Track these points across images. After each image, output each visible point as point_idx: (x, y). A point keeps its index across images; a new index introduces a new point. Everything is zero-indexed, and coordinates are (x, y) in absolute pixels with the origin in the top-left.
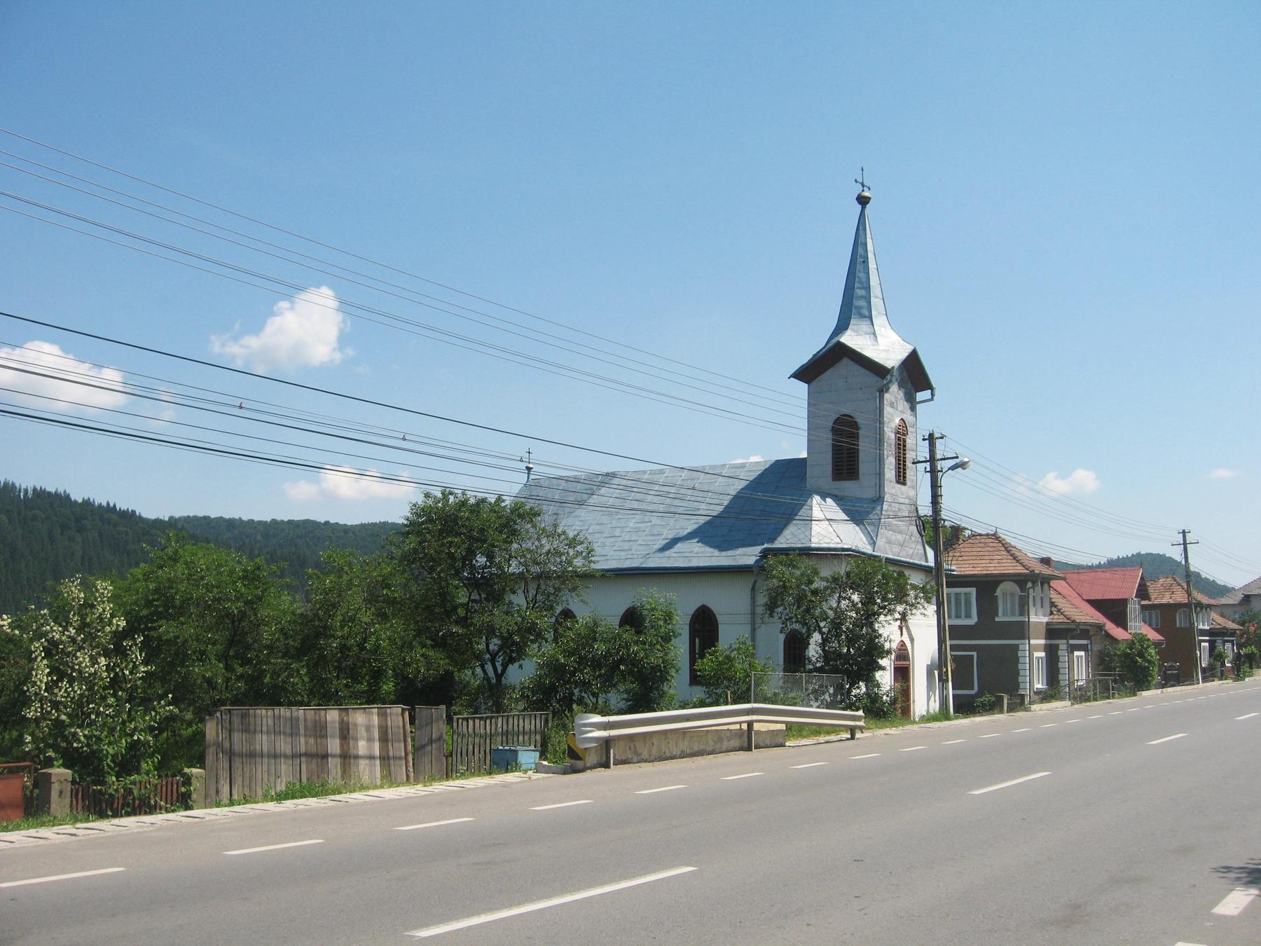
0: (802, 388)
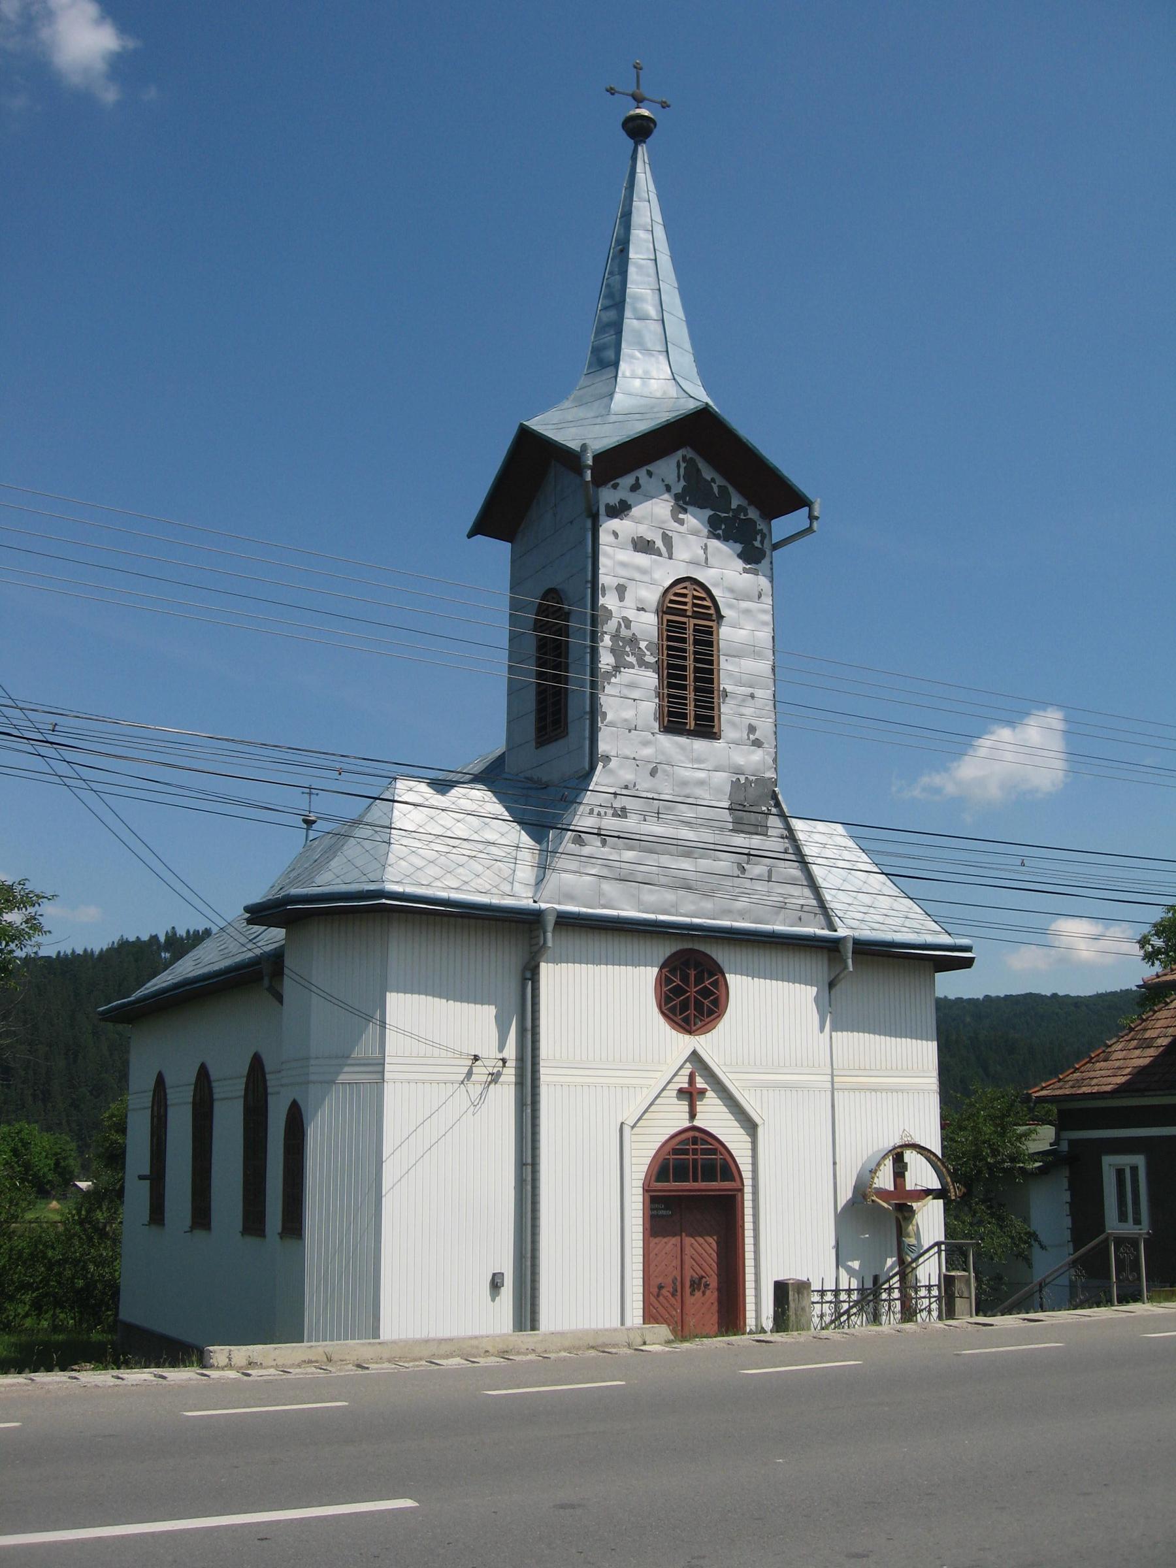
0: (500, 550)
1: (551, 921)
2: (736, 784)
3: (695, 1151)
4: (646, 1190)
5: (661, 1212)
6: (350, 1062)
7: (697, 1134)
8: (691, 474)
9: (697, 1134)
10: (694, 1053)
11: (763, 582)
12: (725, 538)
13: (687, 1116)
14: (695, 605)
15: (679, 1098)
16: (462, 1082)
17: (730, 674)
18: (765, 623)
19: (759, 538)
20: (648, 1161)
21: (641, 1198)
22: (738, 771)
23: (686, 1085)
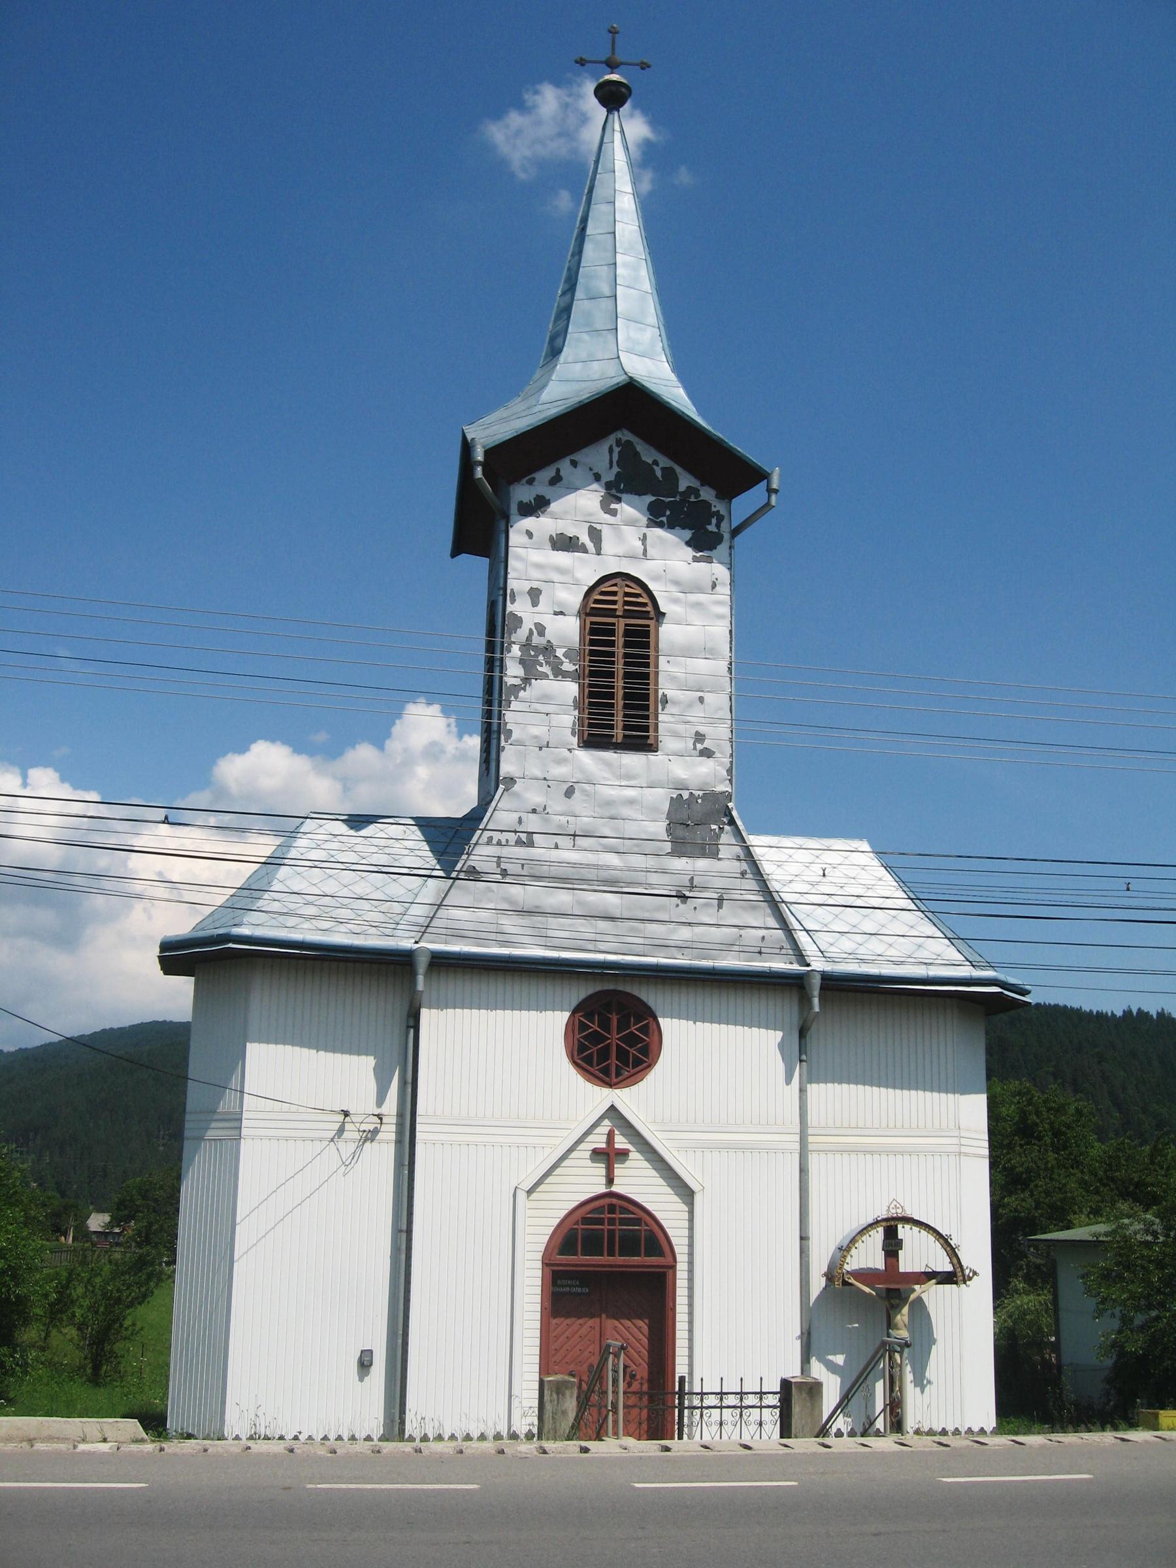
2: (676, 802)
3: (612, 1221)
4: (546, 1263)
6: (216, 1117)
7: (614, 1201)
8: (628, 457)
9: (614, 1201)
10: (612, 1108)
11: (719, 571)
12: (671, 526)
13: (603, 1180)
14: (626, 603)
16: (332, 1140)
17: (673, 679)
18: (720, 617)
19: (714, 521)
20: (550, 1230)
21: (539, 1273)
22: (680, 786)
23: (604, 1146)
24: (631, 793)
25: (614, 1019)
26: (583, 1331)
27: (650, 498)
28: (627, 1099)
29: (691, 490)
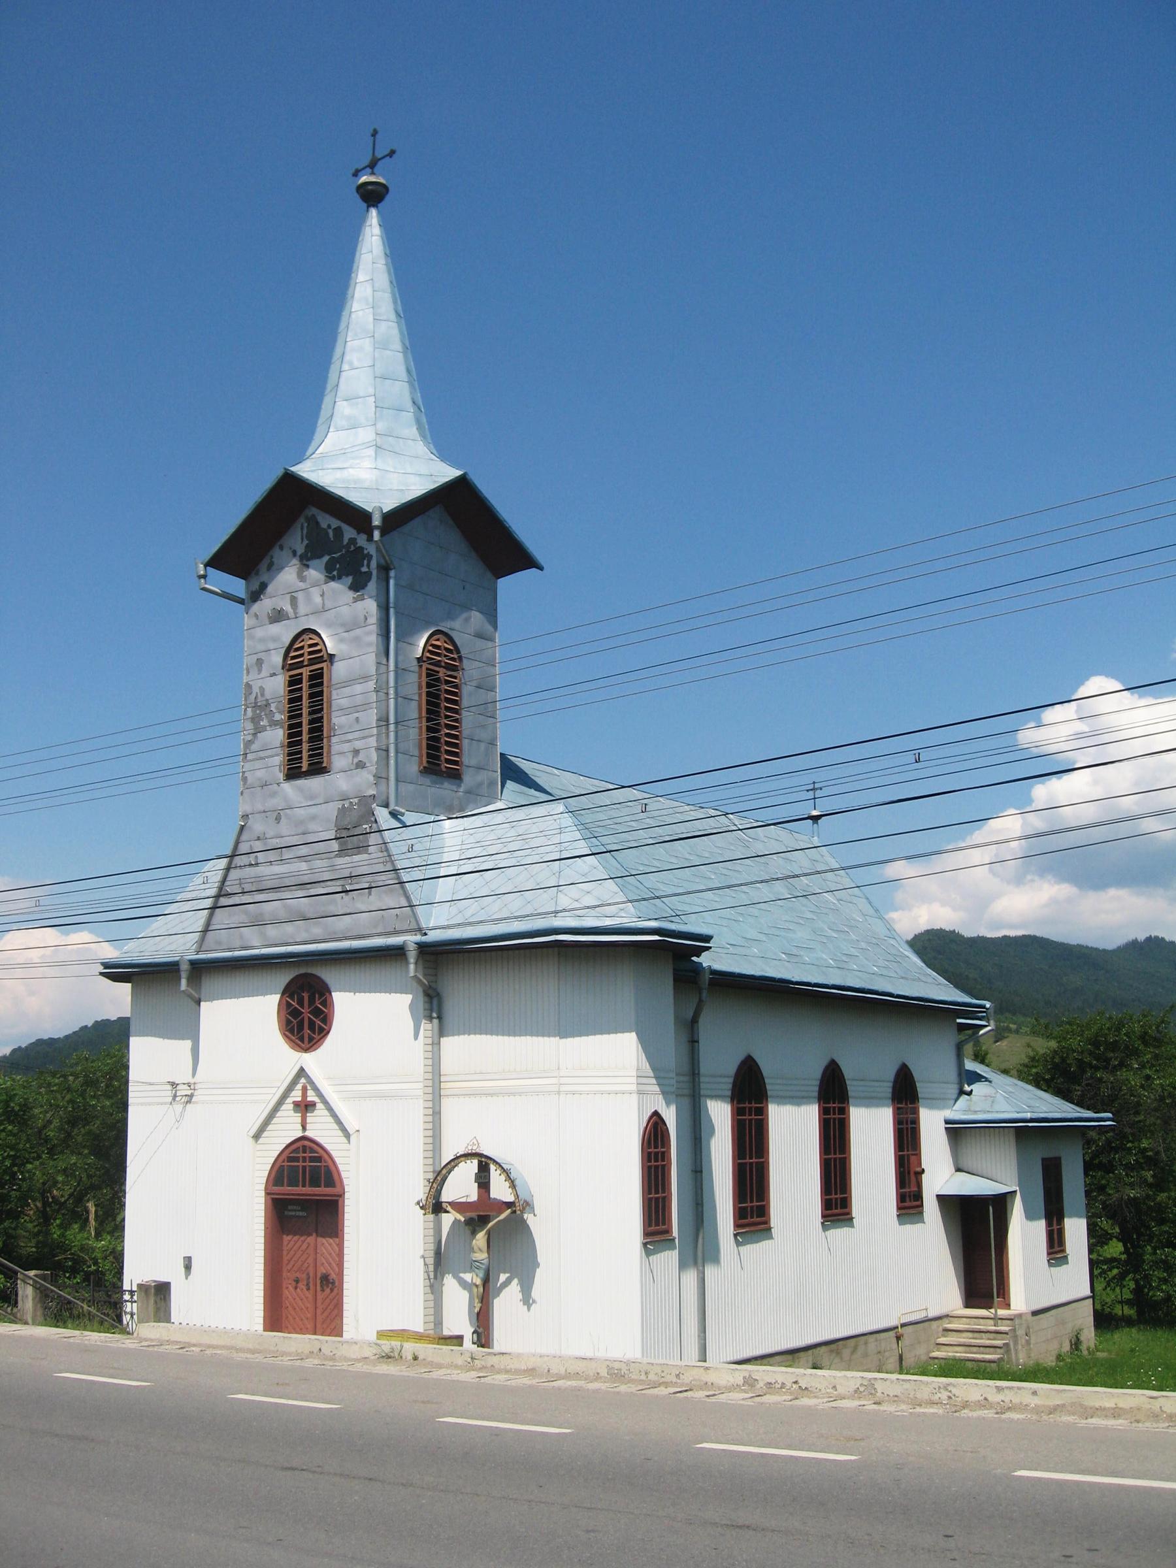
1: (185, 967)
4: (267, 1194)
5: (298, 1213)
7: (307, 1143)
9: (307, 1143)
10: (302, 1070)
15: (295, 1111)
18: (370, 644)
21: (263, 1200)
24: (313, 810)
25: (306, 995)
26: (304, 1246)
27: (326, 558)
28: (311, 1061)
29: (353, 541)
